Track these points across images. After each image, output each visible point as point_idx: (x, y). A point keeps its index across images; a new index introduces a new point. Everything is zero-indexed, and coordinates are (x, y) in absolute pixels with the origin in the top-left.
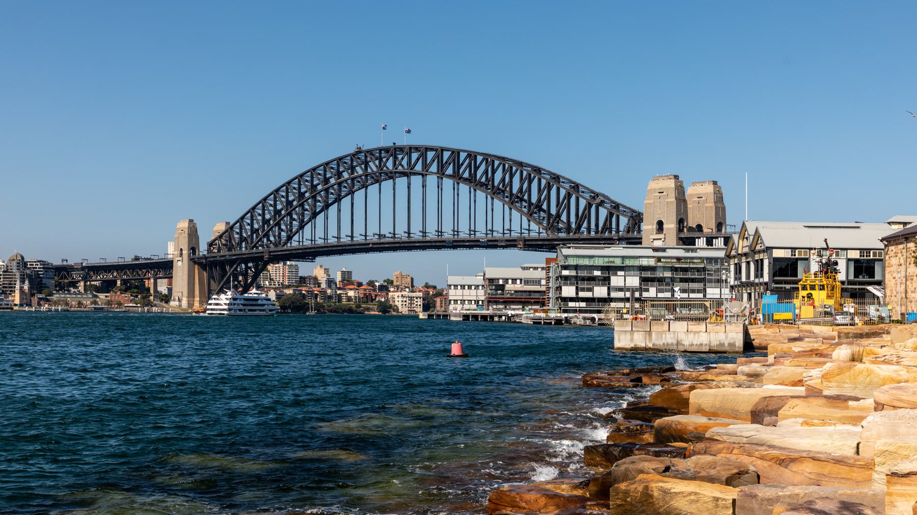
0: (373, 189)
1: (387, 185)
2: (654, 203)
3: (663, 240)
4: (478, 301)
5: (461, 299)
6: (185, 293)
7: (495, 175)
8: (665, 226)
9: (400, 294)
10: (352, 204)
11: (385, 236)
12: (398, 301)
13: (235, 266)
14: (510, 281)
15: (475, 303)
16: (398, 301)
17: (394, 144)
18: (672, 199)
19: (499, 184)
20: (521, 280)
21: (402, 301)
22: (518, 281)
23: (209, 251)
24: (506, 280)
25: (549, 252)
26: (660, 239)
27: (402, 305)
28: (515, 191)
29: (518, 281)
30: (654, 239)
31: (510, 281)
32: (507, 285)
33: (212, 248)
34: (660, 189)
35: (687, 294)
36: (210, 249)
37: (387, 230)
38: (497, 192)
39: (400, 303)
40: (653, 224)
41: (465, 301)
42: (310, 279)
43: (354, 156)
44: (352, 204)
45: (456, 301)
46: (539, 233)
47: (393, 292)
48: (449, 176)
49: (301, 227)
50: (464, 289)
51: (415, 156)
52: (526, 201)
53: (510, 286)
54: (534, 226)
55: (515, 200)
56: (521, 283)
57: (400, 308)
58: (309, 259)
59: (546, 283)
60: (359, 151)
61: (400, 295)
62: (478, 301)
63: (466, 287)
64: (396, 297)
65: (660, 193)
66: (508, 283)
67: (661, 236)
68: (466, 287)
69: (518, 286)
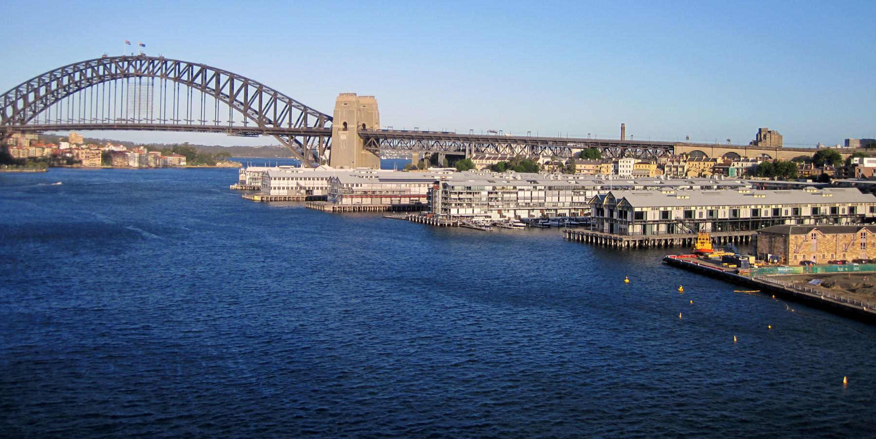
11: (124, 120)
14: (355, 185)
31: (355, 185)
37: (124, 117)
43: (100, 62)
45: (275, 188)
56: (361, 186)
60: (105, 58)
64: (80, 153)
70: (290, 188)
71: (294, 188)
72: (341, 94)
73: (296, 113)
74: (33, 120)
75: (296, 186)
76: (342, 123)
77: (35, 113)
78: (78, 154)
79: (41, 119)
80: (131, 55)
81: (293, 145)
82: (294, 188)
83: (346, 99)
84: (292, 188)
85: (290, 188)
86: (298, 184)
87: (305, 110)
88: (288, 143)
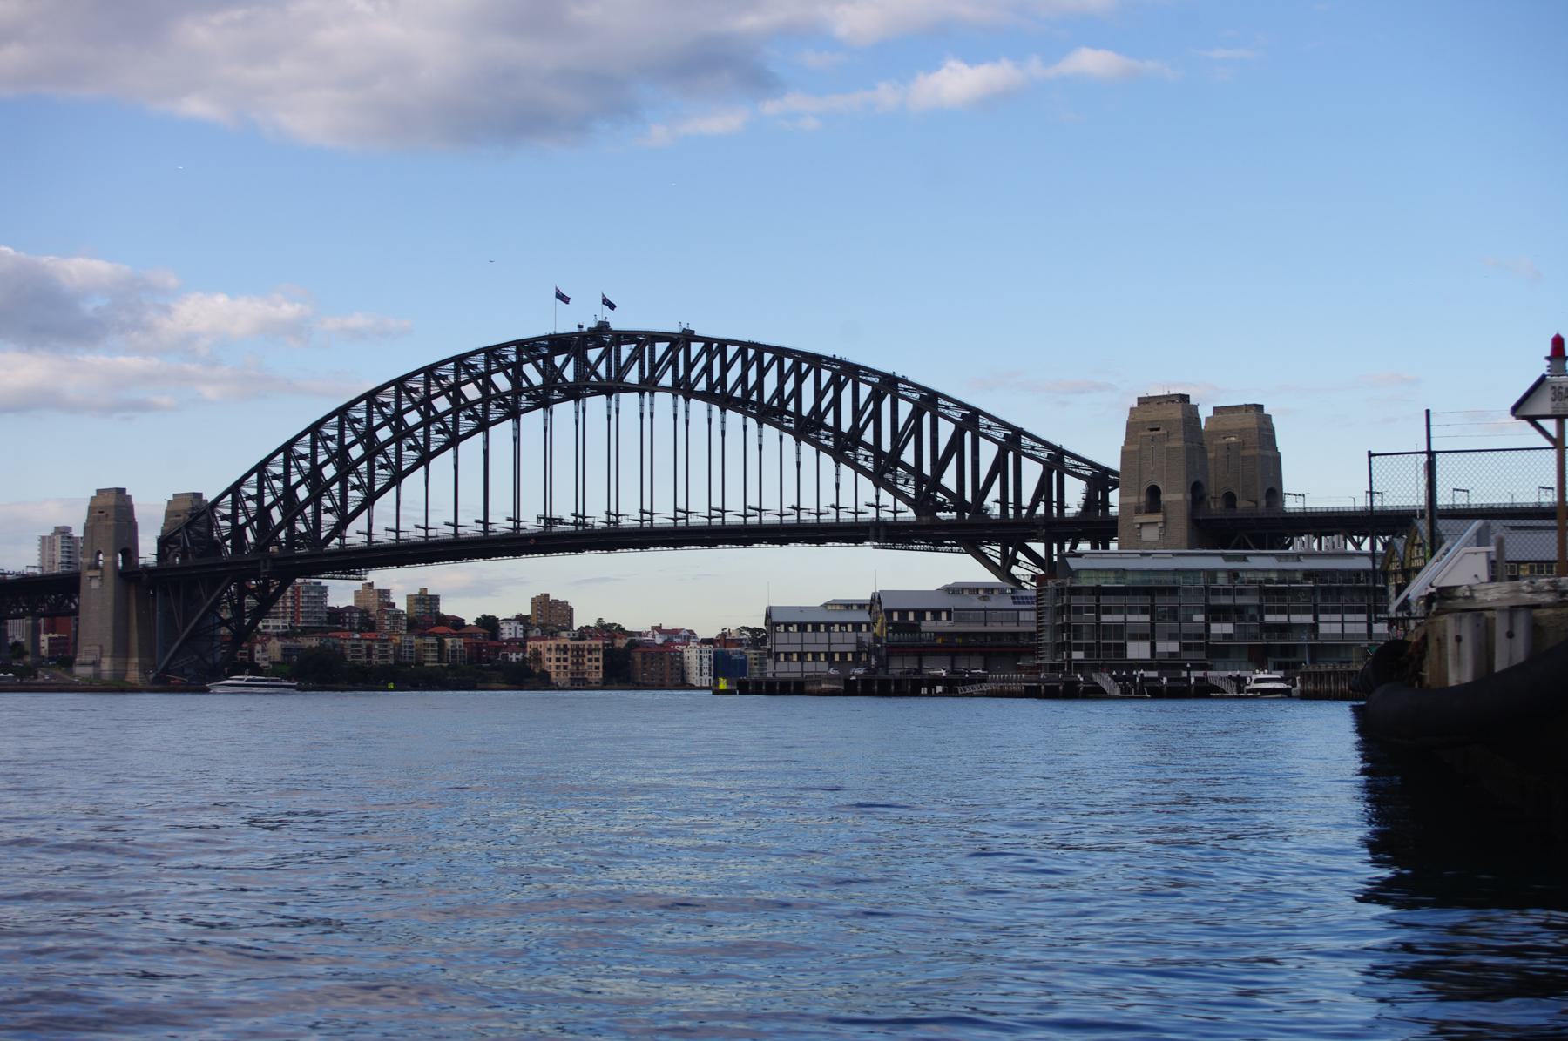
0: (532, 421)
1: (564, 411)
2: (1140, 451)
3: (1161, 525)
4: (833, 653)
5: (800, 650)
6: (108, 646)
7: (776, 386)
8: (1165, 498)
9: (552, 643)
10: (486, 452)
11: (561, 521)
12: (550, 660)
13: (218, 592)
14: (928, 616)
15: (826, 659)
16: (550, 660)
17: (580, 326)
18: (1178, 443)
19: (772, 400)
20: (949, 612)
21: (558, 660)
22: (944, 616)
23: (161, 554)
24: (920, 614)
25: (936, 551)
26: (1156, 523)
27: (558, 667)
28: (806, 411)
29: (944, 616)
30: (1141, 524)
31: (928, 616)
32: (923, 623)
33: (167, 550)
34: (1152, 422)
35: (1346, 631)
36: (164, 551)
37: (564, 509)
38: (767, 414)
39: (554, 663)
40: (1139, 495)
41: (806, 653)
42: (351, 613)
44: (486, 452)
45: (788, 655)
46: (895, 512)
47: (536, 639)
48: (701, 396)
49: (368, 503)
50: (806, 630)
51: (626, 351)
52: (866, 446)
53: (928, 625)
54: (886, 498)
55: (843, 448)
56: (949, 618)
57: (553, 676)
58: (354, 573)
59: (1038, 618)
61: (553, 647)
62: (833, 653)
63: (809, 628)
65: (1152, 430)
66: (924, 618)
67: (1158, 517)
68: (809, 628)
69: (944, 625)
70: (837, 658)
71: (850, 658)
72: (1142, 401)
73: (1032, 472)
74: (337, 540)
75: (853, 648)
76: (1145, 488)
77: (345, 520)
78: (537, 655)
79: (354, 535)
80: (576, 330)
81: (1015, 570)
82: (850, 658)
83: (1154, 414)
84: (843, 655)
85: (837, 658)
86: (860, 643)
87: (1057, 461)
88: (998, 562)
